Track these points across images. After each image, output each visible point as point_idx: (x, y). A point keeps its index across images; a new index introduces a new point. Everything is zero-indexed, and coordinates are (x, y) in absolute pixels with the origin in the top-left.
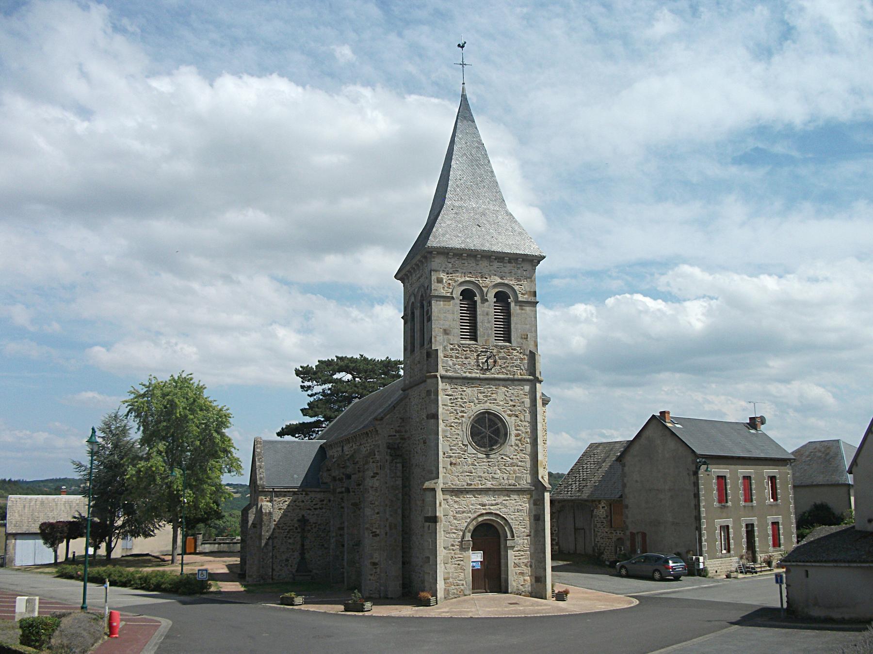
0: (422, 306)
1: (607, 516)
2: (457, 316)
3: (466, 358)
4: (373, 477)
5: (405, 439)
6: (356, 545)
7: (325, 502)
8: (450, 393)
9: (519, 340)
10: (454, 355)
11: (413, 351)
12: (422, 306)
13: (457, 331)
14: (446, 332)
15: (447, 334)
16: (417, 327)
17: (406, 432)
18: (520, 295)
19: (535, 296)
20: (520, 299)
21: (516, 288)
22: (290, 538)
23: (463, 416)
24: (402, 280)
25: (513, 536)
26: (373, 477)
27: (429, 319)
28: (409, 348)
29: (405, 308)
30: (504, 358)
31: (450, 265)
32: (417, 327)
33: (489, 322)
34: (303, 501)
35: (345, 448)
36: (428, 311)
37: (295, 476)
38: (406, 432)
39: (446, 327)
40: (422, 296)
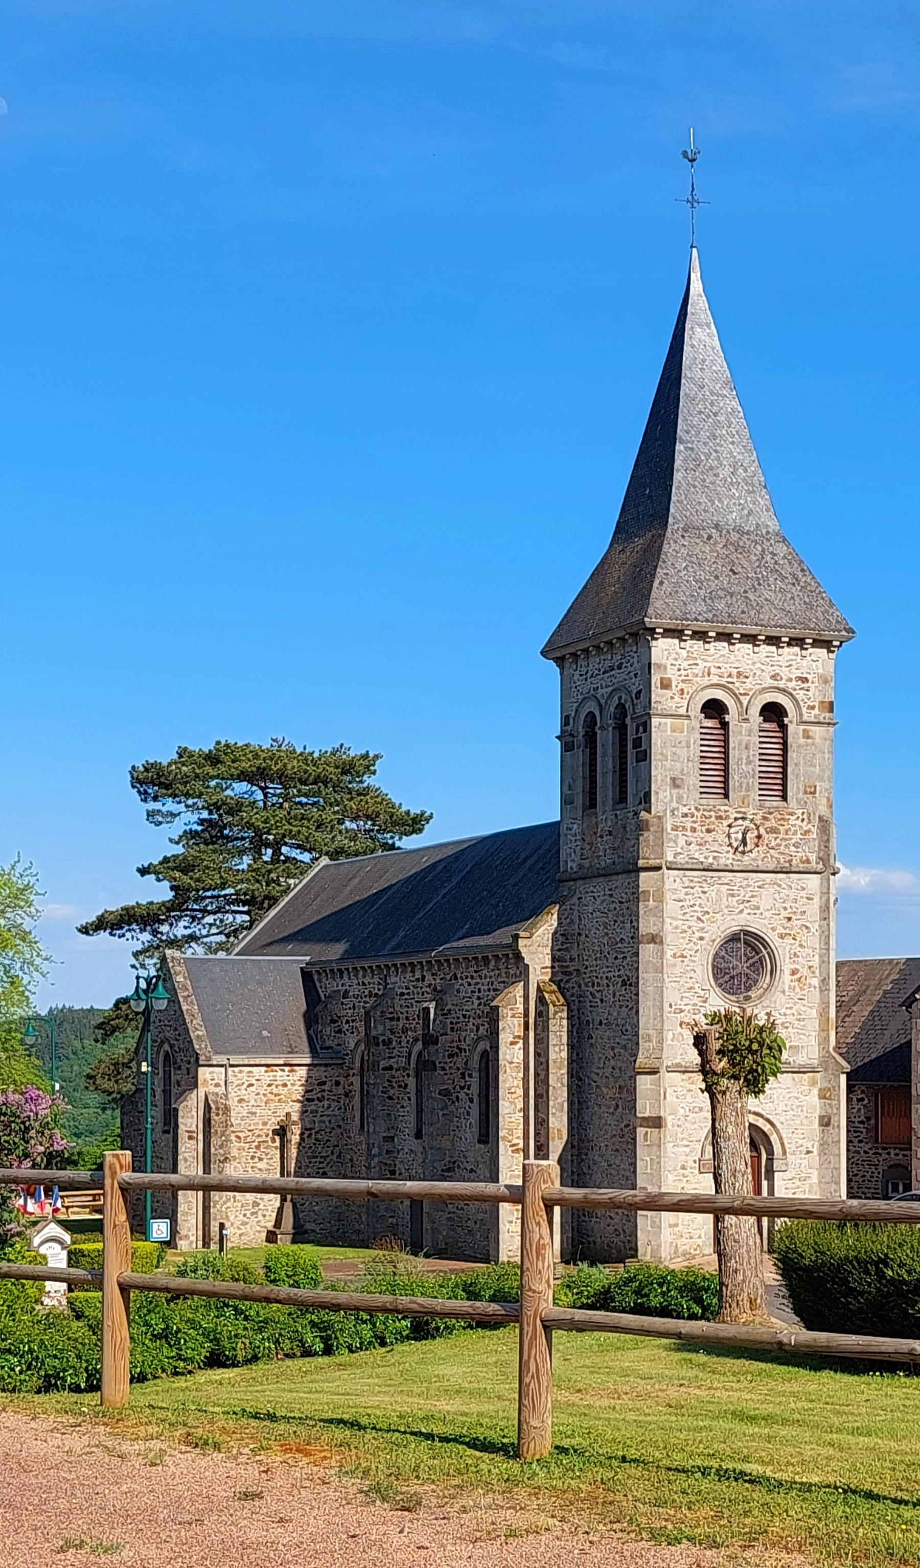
0: (621, 729)
1: (868, 1119)
2: (695, 751)
3: (709, 831)
4: (512, 1043)
5: (571, 974)
6: (448, 1170)
7: (326, 1087)
8: (682, 896)
9: (801, 795)
10: (689, 826)
11: (591, 803)
12: (621, 729)
13: (693, 780)
14: (675, 783)
15: (678, 787)
16: (606, 764)
17: (572, 960)
18: (804, 710)
19: (831, 710)
20: (806, 718)
21: (800, 695)
22: (260, 1159)
23: (701, 939)
24: (560, 661)
25: (784, 1153)
26: (512, 1043)
27: (644, 756)
28: (579, 800)
29: (565, 721)
30: (773, 830)
31: (684, 653)
32: (606, 764)
33: (749, 762)
34: (285, 1085)
35: (392, 979)
36: (637, 742)
37: (265, 1033)
38: (572, 960)
39: (677, 774)
40: (621, 706)
